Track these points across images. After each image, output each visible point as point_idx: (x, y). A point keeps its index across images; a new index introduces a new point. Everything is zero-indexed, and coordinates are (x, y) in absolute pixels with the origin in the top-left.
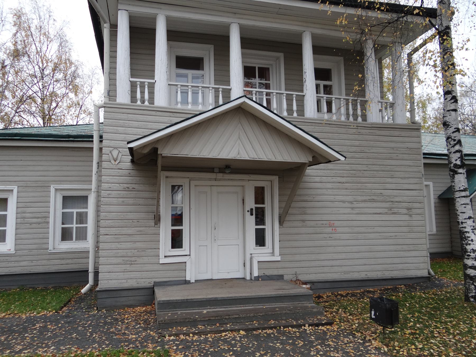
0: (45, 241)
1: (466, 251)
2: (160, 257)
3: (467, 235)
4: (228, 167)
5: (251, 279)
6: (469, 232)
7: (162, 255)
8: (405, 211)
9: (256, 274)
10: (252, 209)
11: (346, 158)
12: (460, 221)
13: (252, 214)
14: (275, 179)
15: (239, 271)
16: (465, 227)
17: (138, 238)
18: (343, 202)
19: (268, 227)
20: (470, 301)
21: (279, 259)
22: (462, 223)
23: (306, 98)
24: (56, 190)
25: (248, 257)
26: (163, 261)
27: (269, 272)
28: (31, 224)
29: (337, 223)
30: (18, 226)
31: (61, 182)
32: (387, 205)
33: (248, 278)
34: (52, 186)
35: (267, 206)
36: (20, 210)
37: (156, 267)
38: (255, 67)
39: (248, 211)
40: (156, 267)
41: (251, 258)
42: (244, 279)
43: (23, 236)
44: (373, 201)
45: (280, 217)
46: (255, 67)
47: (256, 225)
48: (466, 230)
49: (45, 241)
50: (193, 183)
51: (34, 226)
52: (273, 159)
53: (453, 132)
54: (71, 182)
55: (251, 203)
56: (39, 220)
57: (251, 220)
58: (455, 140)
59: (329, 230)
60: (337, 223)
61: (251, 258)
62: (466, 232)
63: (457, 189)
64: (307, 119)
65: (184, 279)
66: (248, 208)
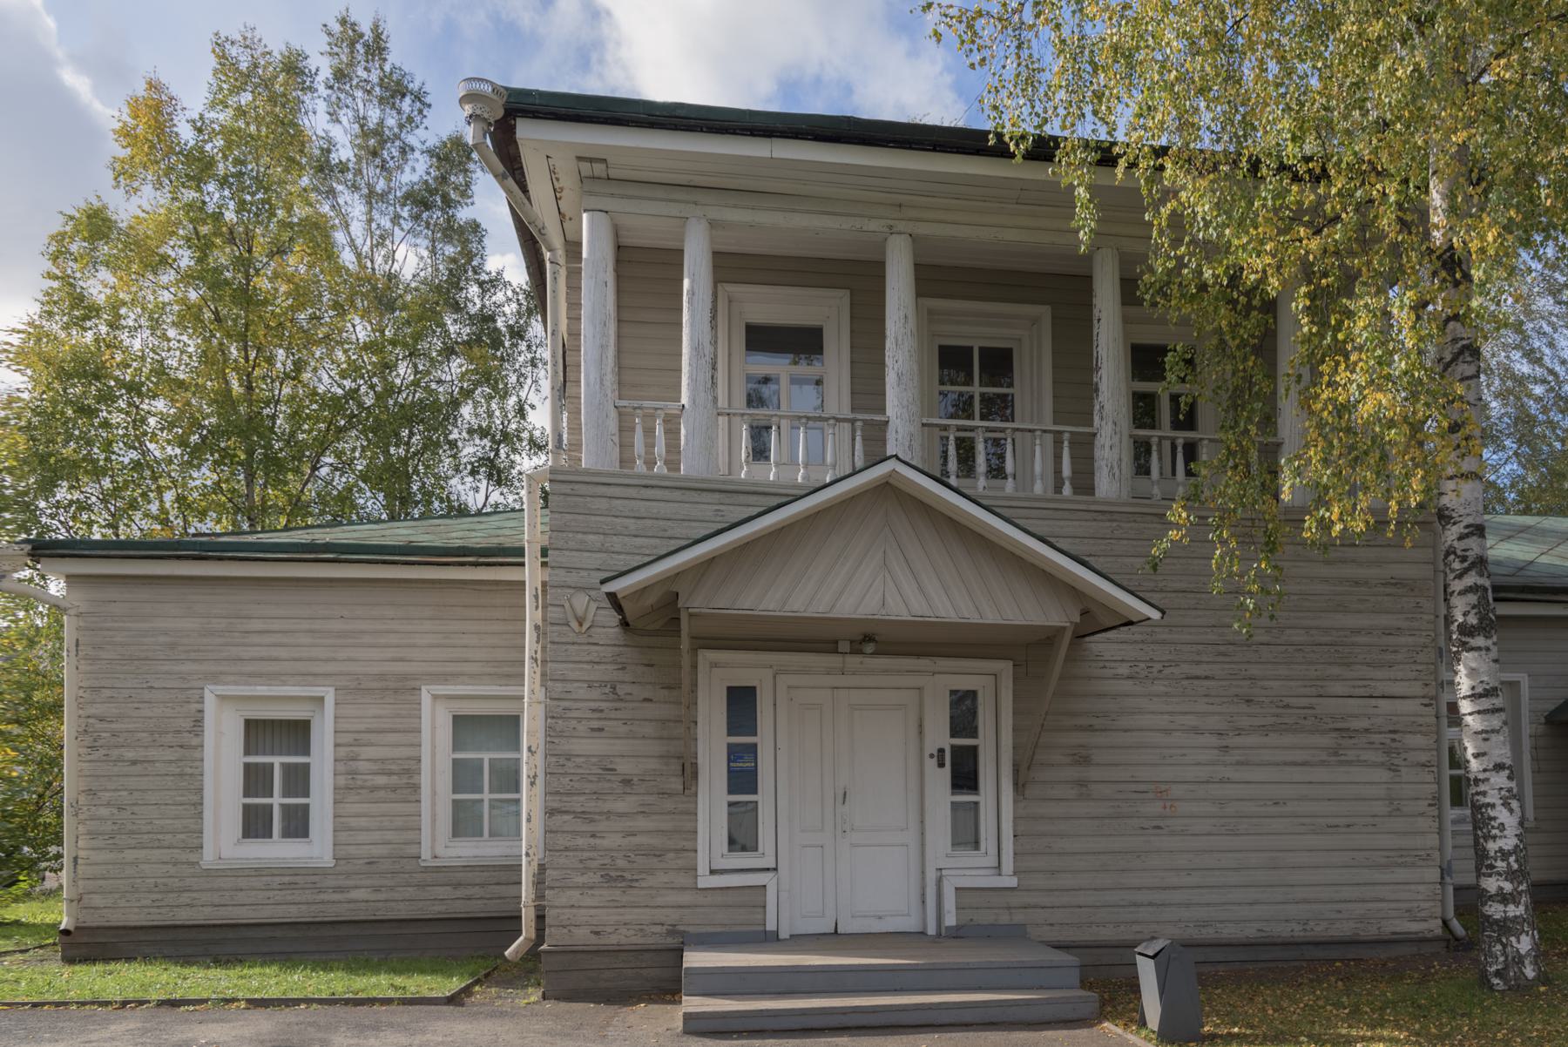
0: (410, 835)
2: (700, 872)
3: (1492, 813)
4: (868, 638)
5: (939, 935)
6: (1493, 806)
7: (703, 868)
9: (950, 920)
10: (941, 751)
11: (1163, 613)
12: (1472, 776)
13: (941, 765)
14: (1005, 668)
15: (908, 915)
16: (1484, 794)
17: (642, 823)
18: (1196, 731)
20: (1491, 987)
21: (1013, 882)
22: (1477, 781)
23: (1099, 441)
24: (435, 697)
25: (931, 876)
26: (705, 881)
27: (985, 918)
28: (374, 789)
29: (1177, 791)
30: (341, 793)
31: (444, 678)
33: (931, 930)
34: (423, 688)
35: (984, 742)
36: (343, 751)
37: (686, 898)
38: (971, 349)
39: (932, 756)
40: (686, 898)
41: (939, 881)
42: (923, 933)
43: (353, 822)
46: (971, 349)
47: (730, 734)
48: (1487, 800)
49: (410, 835)
50: (784, 681)
51: (382, 794)
52: (975, 619)
53: (1461, 538)
54: (474, 678)
55: (940, 736)
56: (394, 780)
57: (940, 779)
58: (1464, 559)
59: (1155, 808)
60: (1177, 791)
61: (939, 881)
62: (1488, 805)
65: (761, 928)
66: (931, 747)
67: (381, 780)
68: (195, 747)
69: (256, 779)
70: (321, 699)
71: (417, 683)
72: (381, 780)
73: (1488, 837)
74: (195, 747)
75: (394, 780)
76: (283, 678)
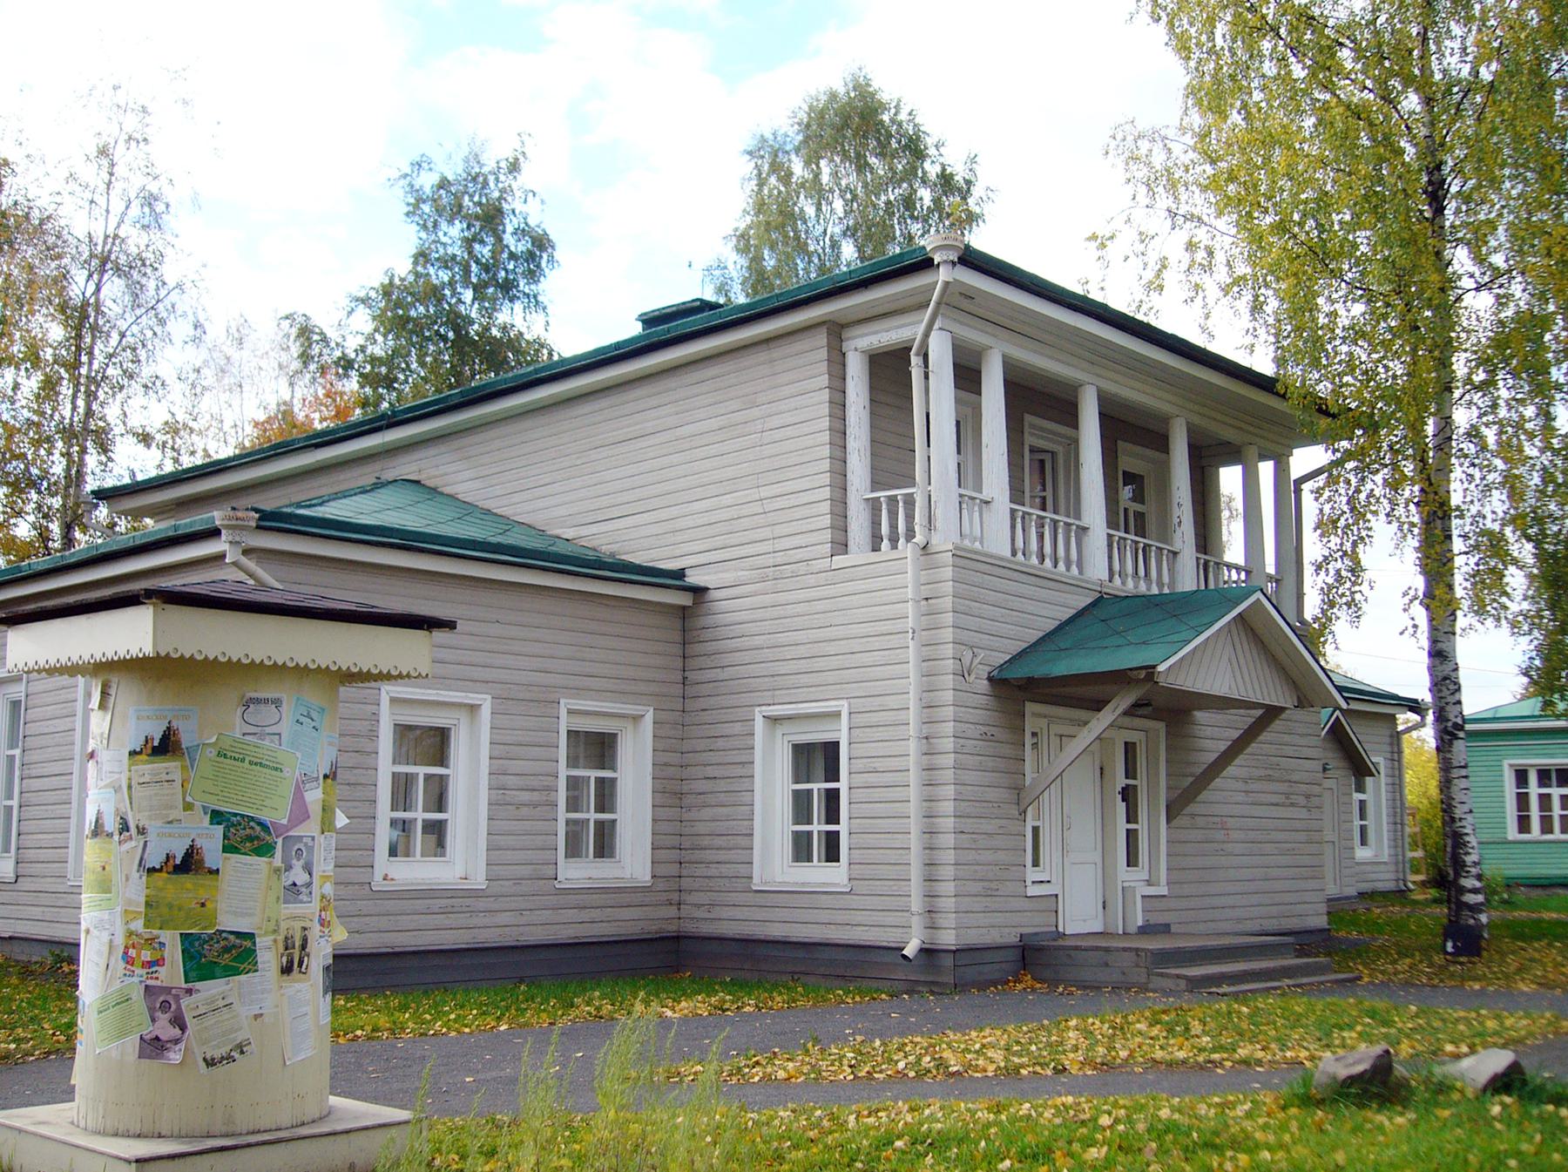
0: (548, 855)
1: (1463, 864)
3: (1467, 838)
8: (1302, 800)
16: (1463, 827)
19: (1142, 827)
21: (1164, 891)
22: (1461, 819)
26: (1033, 891)
28: (519, 806)
31: (579, 692)
32: (1283, 787)
34: (562, 701)
44: (1269, 779)
45: (1167, 807)
48: (1466, 831)
51: (525, 811)
54: (599, 693)
59: (1220, 835)
60: (1231, 822)
62: (1467, 834)
63: (1456, 764)
64: (1087, 582)
67: (525, 796)
68: (369, 753)
69: (402, 790)
70: (473, 709)
71: (552, 697)
72: (525, 796)
73: (1468, 853)
74: (369, 753)
75: (535, 796)
76: (447, 681)
